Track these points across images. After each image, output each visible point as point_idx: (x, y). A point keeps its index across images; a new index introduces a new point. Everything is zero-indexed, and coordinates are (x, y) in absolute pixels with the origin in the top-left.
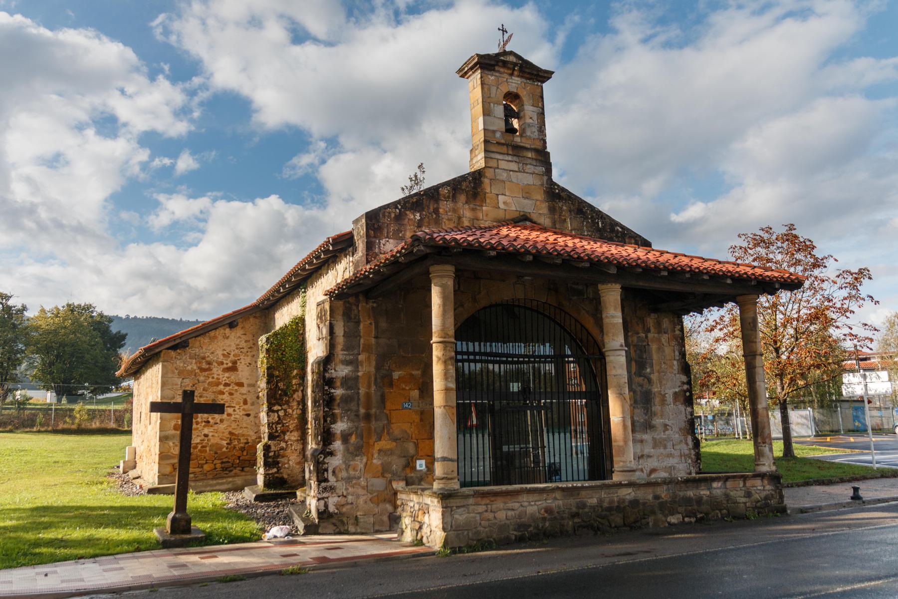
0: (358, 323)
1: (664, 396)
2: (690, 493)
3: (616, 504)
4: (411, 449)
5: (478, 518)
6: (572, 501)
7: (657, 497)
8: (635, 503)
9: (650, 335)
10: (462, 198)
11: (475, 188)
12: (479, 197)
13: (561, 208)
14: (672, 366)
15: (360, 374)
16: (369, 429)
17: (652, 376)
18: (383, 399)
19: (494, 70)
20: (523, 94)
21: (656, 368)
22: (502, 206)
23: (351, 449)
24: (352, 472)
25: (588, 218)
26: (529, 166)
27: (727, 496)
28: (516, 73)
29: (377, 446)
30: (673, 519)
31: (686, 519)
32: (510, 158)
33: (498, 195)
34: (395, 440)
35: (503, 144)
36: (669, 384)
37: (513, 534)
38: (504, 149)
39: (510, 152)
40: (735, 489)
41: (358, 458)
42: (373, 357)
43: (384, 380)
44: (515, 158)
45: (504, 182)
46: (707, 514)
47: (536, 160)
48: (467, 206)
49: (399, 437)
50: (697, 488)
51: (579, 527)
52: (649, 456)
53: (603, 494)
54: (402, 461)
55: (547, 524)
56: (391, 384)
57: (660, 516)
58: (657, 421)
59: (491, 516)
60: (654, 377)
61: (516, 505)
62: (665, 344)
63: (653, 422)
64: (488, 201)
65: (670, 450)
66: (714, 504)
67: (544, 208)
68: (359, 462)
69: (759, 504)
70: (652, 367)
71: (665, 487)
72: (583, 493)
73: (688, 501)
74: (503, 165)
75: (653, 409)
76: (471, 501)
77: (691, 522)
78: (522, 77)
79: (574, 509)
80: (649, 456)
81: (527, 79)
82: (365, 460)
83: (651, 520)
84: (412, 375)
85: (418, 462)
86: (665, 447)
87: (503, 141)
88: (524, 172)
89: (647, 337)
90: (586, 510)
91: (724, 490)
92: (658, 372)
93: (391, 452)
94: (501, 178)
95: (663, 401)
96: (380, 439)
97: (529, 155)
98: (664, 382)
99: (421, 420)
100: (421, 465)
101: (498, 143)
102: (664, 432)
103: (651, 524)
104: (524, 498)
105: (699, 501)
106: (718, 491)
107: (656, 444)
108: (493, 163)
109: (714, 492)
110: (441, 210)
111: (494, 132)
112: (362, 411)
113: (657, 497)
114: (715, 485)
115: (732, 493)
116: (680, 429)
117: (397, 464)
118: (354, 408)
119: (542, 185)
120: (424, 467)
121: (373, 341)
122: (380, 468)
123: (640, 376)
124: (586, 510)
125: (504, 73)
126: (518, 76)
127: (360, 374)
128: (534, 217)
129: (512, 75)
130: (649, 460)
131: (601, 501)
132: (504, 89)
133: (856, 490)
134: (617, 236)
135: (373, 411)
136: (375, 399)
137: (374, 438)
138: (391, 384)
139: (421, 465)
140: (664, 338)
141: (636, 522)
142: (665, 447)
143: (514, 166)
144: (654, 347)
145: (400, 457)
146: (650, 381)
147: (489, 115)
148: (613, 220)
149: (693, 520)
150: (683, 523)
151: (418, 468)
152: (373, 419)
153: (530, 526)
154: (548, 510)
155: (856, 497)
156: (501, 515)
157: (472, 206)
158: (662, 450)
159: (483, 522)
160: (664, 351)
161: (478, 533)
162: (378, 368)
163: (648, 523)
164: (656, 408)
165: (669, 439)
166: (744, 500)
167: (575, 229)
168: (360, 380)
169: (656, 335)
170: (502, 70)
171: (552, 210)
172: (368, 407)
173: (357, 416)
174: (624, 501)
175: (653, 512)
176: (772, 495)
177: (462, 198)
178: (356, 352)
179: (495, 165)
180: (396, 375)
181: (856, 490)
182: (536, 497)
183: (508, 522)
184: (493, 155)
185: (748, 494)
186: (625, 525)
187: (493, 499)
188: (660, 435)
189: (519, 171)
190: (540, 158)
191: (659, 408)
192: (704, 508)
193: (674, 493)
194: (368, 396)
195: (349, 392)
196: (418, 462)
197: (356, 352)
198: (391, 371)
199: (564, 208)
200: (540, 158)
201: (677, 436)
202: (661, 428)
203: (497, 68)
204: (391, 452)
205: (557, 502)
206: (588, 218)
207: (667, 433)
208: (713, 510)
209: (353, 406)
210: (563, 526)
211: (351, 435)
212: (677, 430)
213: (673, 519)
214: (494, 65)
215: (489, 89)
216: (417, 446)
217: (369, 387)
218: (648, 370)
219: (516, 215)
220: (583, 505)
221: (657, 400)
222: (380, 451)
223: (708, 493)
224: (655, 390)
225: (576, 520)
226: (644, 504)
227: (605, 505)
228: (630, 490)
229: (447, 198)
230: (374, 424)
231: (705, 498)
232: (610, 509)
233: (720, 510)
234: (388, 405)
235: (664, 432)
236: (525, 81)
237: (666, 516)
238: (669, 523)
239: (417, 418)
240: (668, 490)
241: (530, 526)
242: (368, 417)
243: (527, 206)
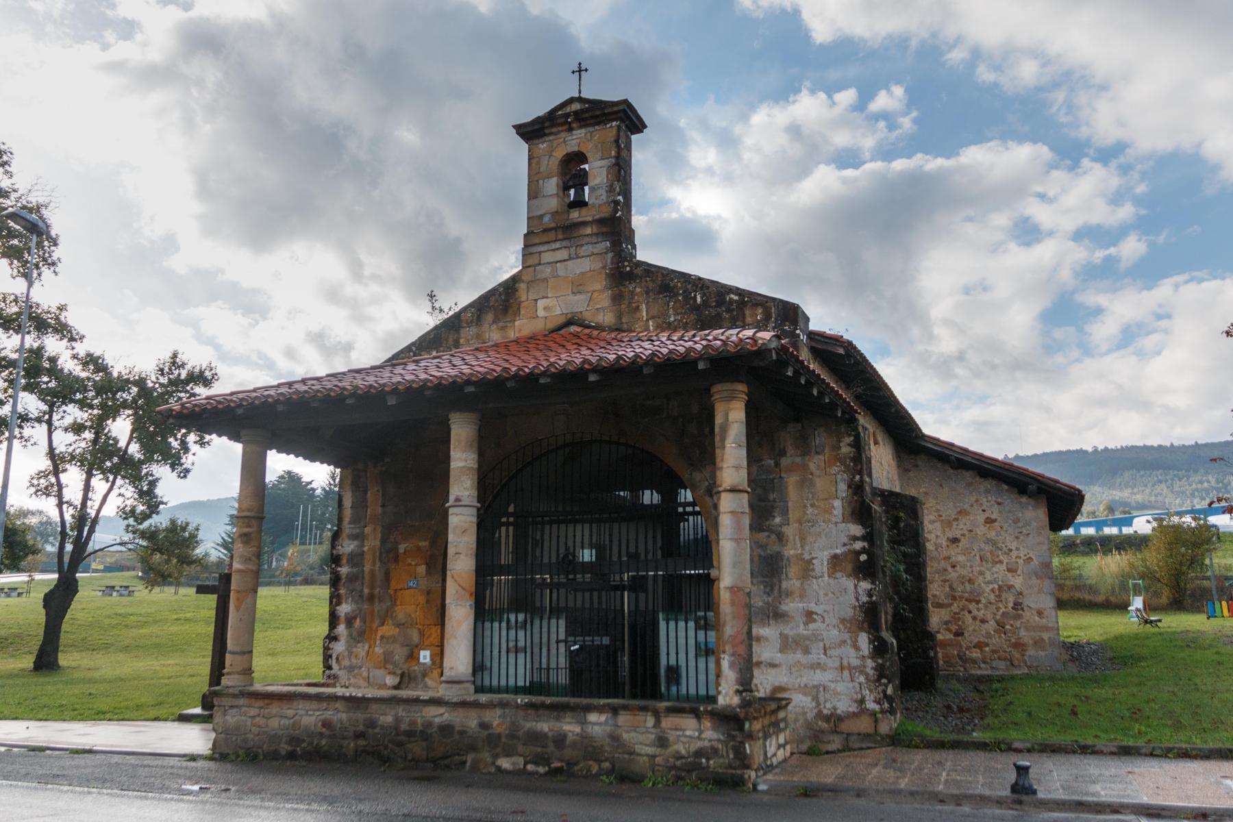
0: (365, 492)
1: (810, 562)
2: (544, 726)
3: (420, 728)
4: (415, 637)
5: (249, 723)
6: (360, 716)
7: (484, 726)
8: (446, 729)
9: (784, 461)
10: (489, 317)
11: (507, 300)
12: (510, 311)
13: (632, 293)
14: (829, 510)
15: (365, 549)
16: (373, 611)
17: (784, 529)
18: (387, 577)
19: (545, 135)
20: (588, 150)
21: (793, 515)
22: (541, 313)
23: (355, 634)
24: (354, 661)
25: (677, 295)
26: (584, 248)
27: (615, 738)
28: (574, 125)
29: (380, 633)
30: (505, 763)
31: (530, 767)
32: (558, 245)
33: (536, 300)
34: (399, 625)
35: (551, 229)
36: (822, 542)
37: (284, 748)
38: (552, 235)
39: (560, 237)
40: (634, 728)
41: (360, 645)
42: (379, 529)
43: (389, 554)
44: (565, 243)
45: (546, 280)
46: (571, 764)
47: (597, 234)
48: (494, 327)
49: (403, 621)
50: (558, 719)
51: (363, 751)
52: (772, 665)
53: (401, 711)
54: (405, 651)
55: (324, 742)
56: (396, 559)
57: (486, 756)
58: (791, 606)
59: (261, 721)
60: (790, 531)
61: (290, 713)
62: (816, 472)
63: (784, 608)
64: (523, 312)
65: (816, 655)
66: (590, 750)
67: (604, 300)
68: (361, 650)
69: (678, 763)
70: (785, 512)
71: (498, 712)
72: (374, 707)
73: (535, 737)
74: (547, 257)
75: (784, 585)
76: (242, 701)
77: (532, 774)
78: (586, 126)
79: (361, 728)
80: (772, 665)
81: (593, 125)
82: (367, 647)
83: (470, 758)
84: (419, 548)
85: (422, 653)
86: (806, 651)
87: (553, 225)
88: (578, 257)
89: (777, 464)
90: (377, 730)
91: (608, 729)
92: (800, 522)
93: (393, 640)
94: (543, 276)
95: (807, 570)
96: (383, 624)
97: (588, 231)
98: (810, 539)
99: (427, 602)
100: (425, 657)
101: (546, 231)
102: (806, 624)
103: (468, 764)
104: (301, 705)
105: (560, 740)
106: (596, 728)
107: (787, 644)
108: (533, 260)
109: (589, 729)
110: (462, 341)
111: (541, 217)
112: (366, 591)
113: (484, 726)
114: (593, 717)
115: (625, 736)
116: (843, 621)
117: (399, 653)
118: (359, 588)
119: (604, 267)
120: (428, 660)
121: (380, 510)
122: (382, 658)
123: (762, 530)
124: (377, 730)
125: (559, 132)
126: (580, 127)
127: (365, 549)
128: (589, 317)
129: (571, 129)
130: (772, 671)
131: (398, 720)
132: (560, 154)
133: (1022, 771)
134: (729, 310)
135: (377, 591)
136: (379, 576)
137: (377, 622)
138: (396, 559)
139: (425, 657)
140: (815, 463)
141: (445, 757)
142: (806, 651)
143: (563, 254)
144: (792, 480)
145: (402, 645)
146: (780, 537)
147: (536, 197)
148: (724, 286)
149: (541, 770)
150: (523, 772)
151: (422, 660)
152: (376, 600)
153: (304, 741)
154: (326, 724)
155: (1022, 790)
156: (274, 723)
157: (501, 324)
158: (799, 656)
159: (253, 729)
160: (812, 485)
161: (245, 741)
162: (383, 541)
163: (464, 763)
164: (791, 582)
165: (816, 637)
166: (651, 750)
167: (653, 318)
168: (366, 556)
169: (798, 460)
170: (554, 130)
171: (617, 299)
172: (372, 587)
173: (361, 596)
174: (429, 724)
175: (473, 748)
176: (715, 751)
177: (489, 317)
178: (362, 524)
179: (537, 262)
180: (402, 548)
181: (1022, 771)
182: (314, 705)
183: (280, 732)
184: (534, 249)
185: (662, 742)
186: (427, 760)
187: (266, 701)
188: (797, 629)
189: (570, 259)
190: (604, 230)
191: (798, 583)
192: (568, 753)
193: (513, 723)
194: (372, 573)
195: (355, 570)
196: (422, 653)
197: (362, 524)
198: (397, 543)
199: (638, 290)
200: (604, 230)
201: (835, 632)
202: (801, 620)
203: (547, 131)
204: (393, 640)
205: (340, 715)
206: (677, 295)
207: (812, 626)
208: (585, 758)
209: (357, 585)
210: (341, 747)
211: (355, 618)
212: (835, 622)
213: (505, 763)
214: (542, 129)
215: (538, 163)
216: (422, 634)
217: (374, 564)
218: (777, 520)
219: (562, 320)
220: (371, 724)
221: (793, 571)
222: (382, 637)
223: (577, 729)
224: (789, 552)
225: (361, 742)
226: (462, 733)
227: (403, 727)
228: (441, 710)
229: (469, 324)
230: (377, 607)
231: (570, 737)
232: (410, 734)
233: (599, 761)
234: (393, 585)
235: (806, 624)
236: (591, 129)
237: (497, 756)
238: (499, 769)
239: (422, 599)
240: (503, 716)
241: (304, 741)
242: (371, 598)
243: (578, 304)
